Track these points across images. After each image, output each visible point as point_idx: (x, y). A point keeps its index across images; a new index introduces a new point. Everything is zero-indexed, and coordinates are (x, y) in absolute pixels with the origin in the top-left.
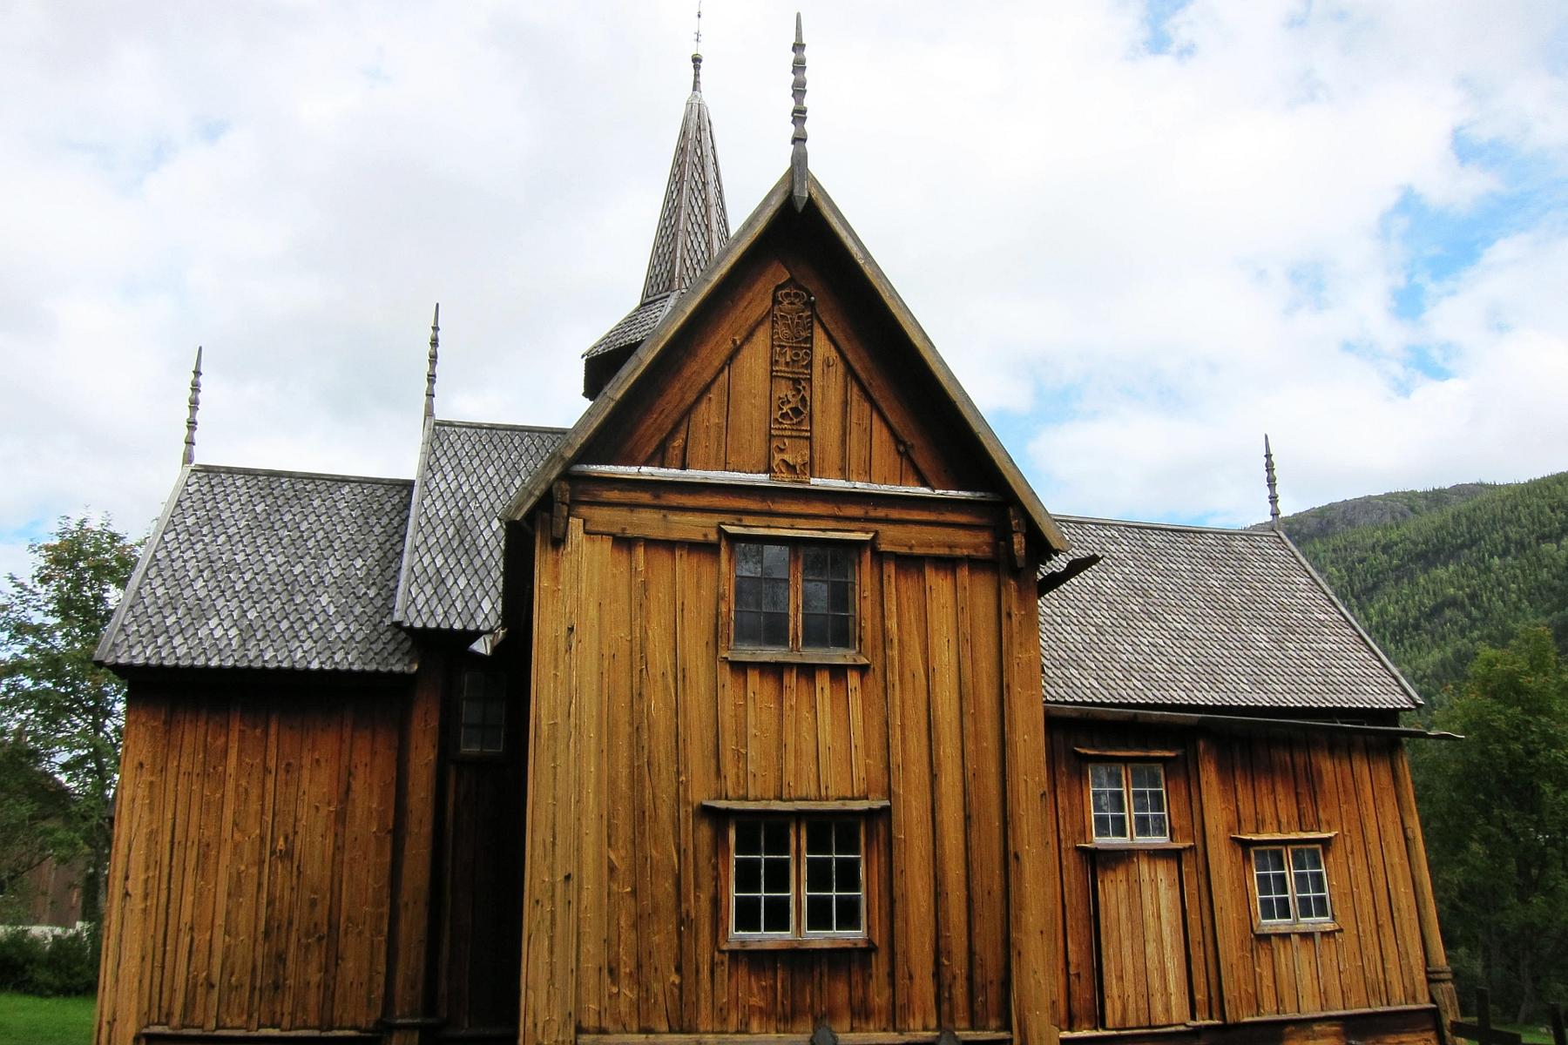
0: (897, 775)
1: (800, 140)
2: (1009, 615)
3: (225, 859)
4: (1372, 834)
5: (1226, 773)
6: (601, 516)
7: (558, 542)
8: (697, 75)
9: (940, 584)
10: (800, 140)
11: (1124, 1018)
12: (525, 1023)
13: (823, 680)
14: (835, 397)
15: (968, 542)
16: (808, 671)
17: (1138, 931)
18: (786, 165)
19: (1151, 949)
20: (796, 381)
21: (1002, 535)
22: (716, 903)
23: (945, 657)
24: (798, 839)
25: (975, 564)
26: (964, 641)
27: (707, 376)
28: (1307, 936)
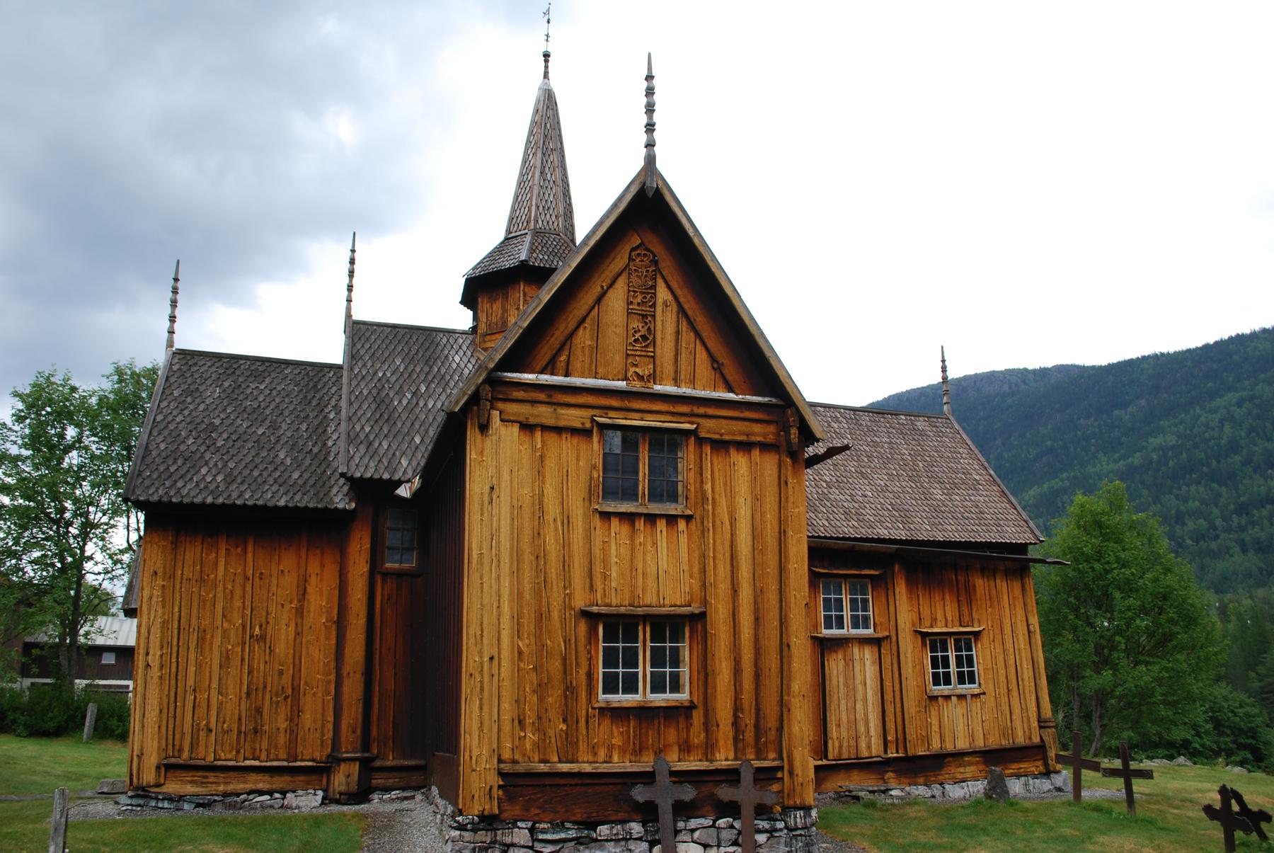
0: (710, 590)
1: (650, 145)
2: (786, 483)
3: (217, 641)
4: (1007, 629)
5: (911, 585)
6: (512, 408)
7: (484, 428)
8: (546, 67)
10: (650, 145)
11: (840, 752)
12: (464, 757)
13: (661, 525)
14: (670, 329)
15: (760, 432)
16: (651, 519)
17: (851, 694)
18: (640, 164)
19: (859, 706)
20: (644, 316)
21: (786, 428)
22: (590, 676)
23: (744, 513)
24: (644, 633)
25: (765, 447)
26: (757, 499)
27: (583, 311)
28: (961, 697)
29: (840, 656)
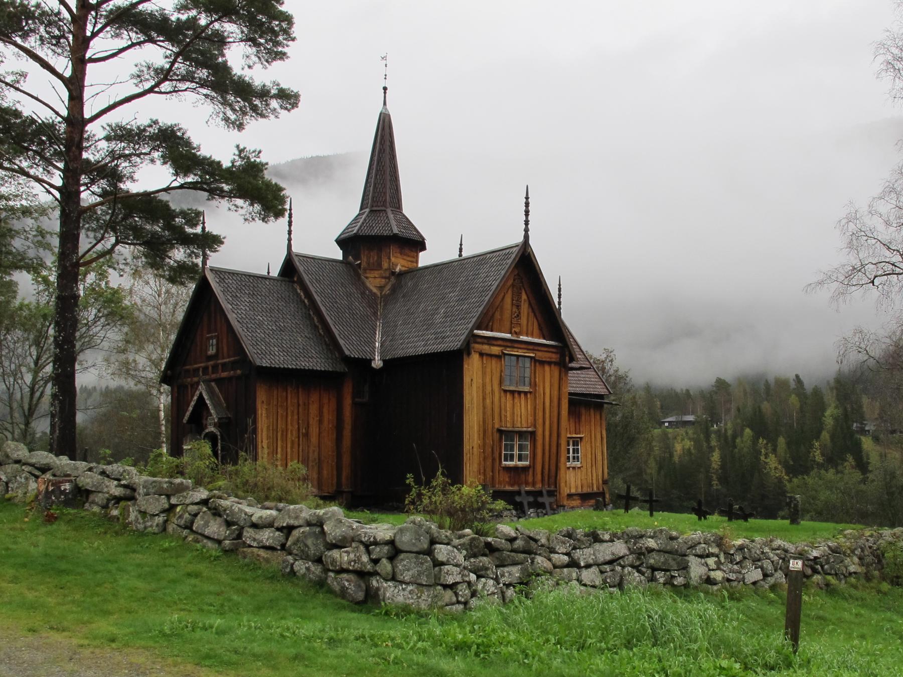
1: (526, 230)
3: (289, 435)
6: (477, 346)
7: (469, 354)
9: (547, 368)
13: (522, 395)
16: (519, 393)
24: (516, 439)
25: (556, 363)
26: (551, 386)
28: (574, 468)
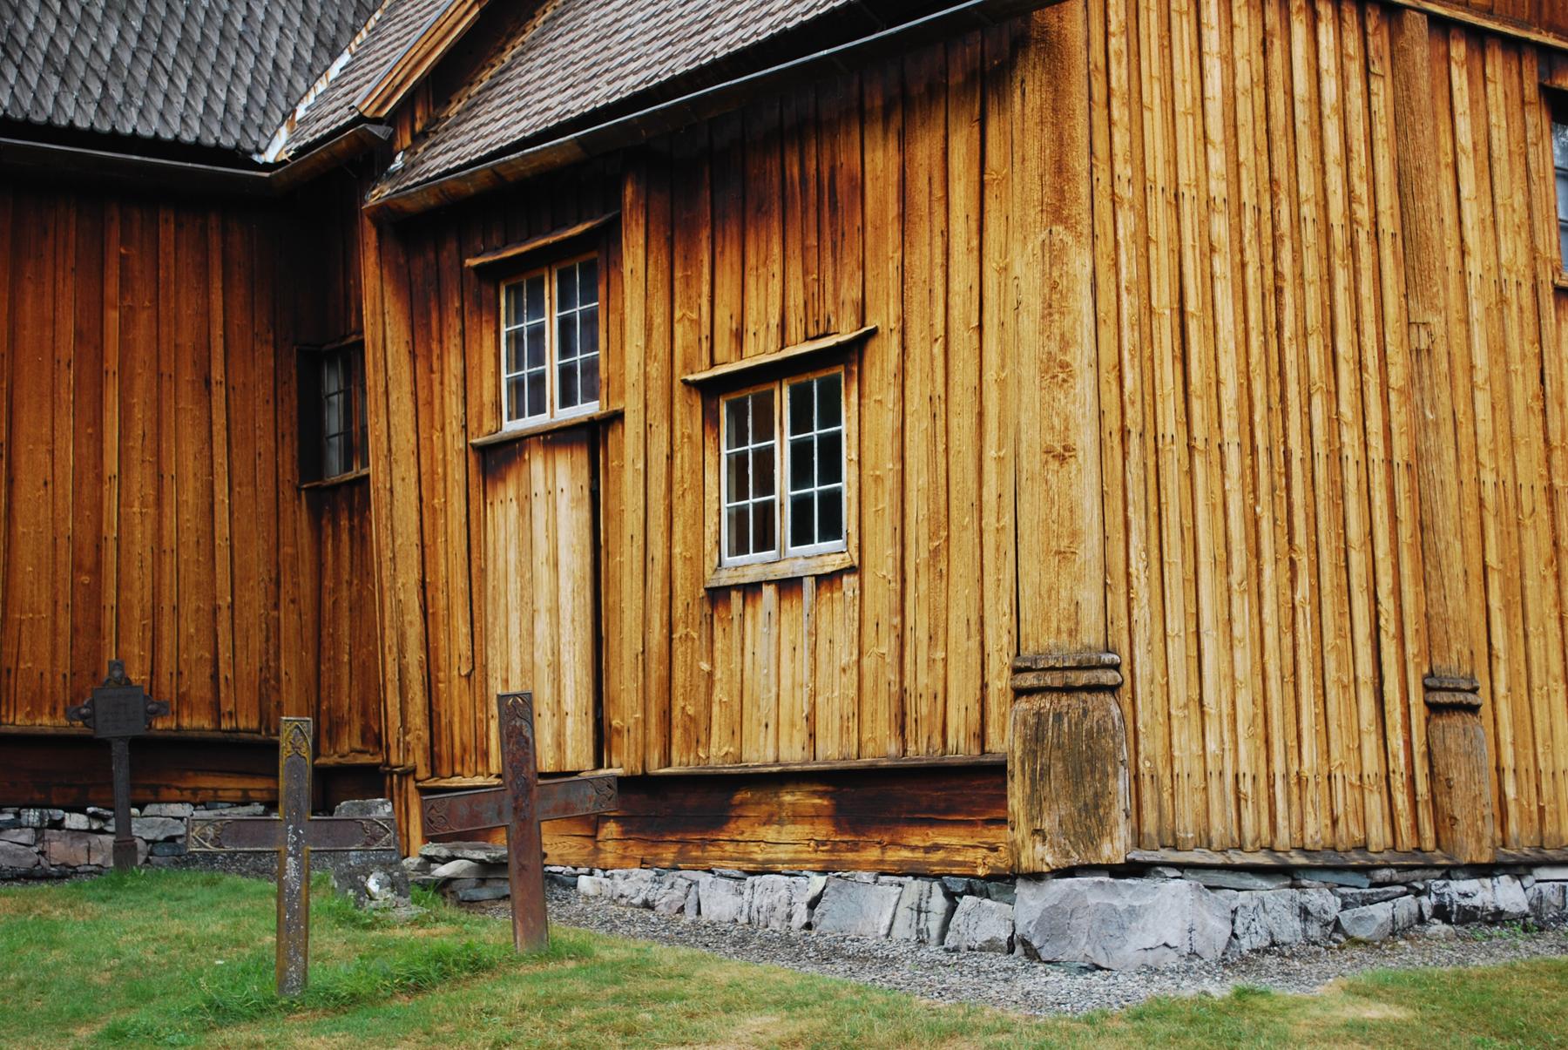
28: (788, 586)
29: (511, 492)
